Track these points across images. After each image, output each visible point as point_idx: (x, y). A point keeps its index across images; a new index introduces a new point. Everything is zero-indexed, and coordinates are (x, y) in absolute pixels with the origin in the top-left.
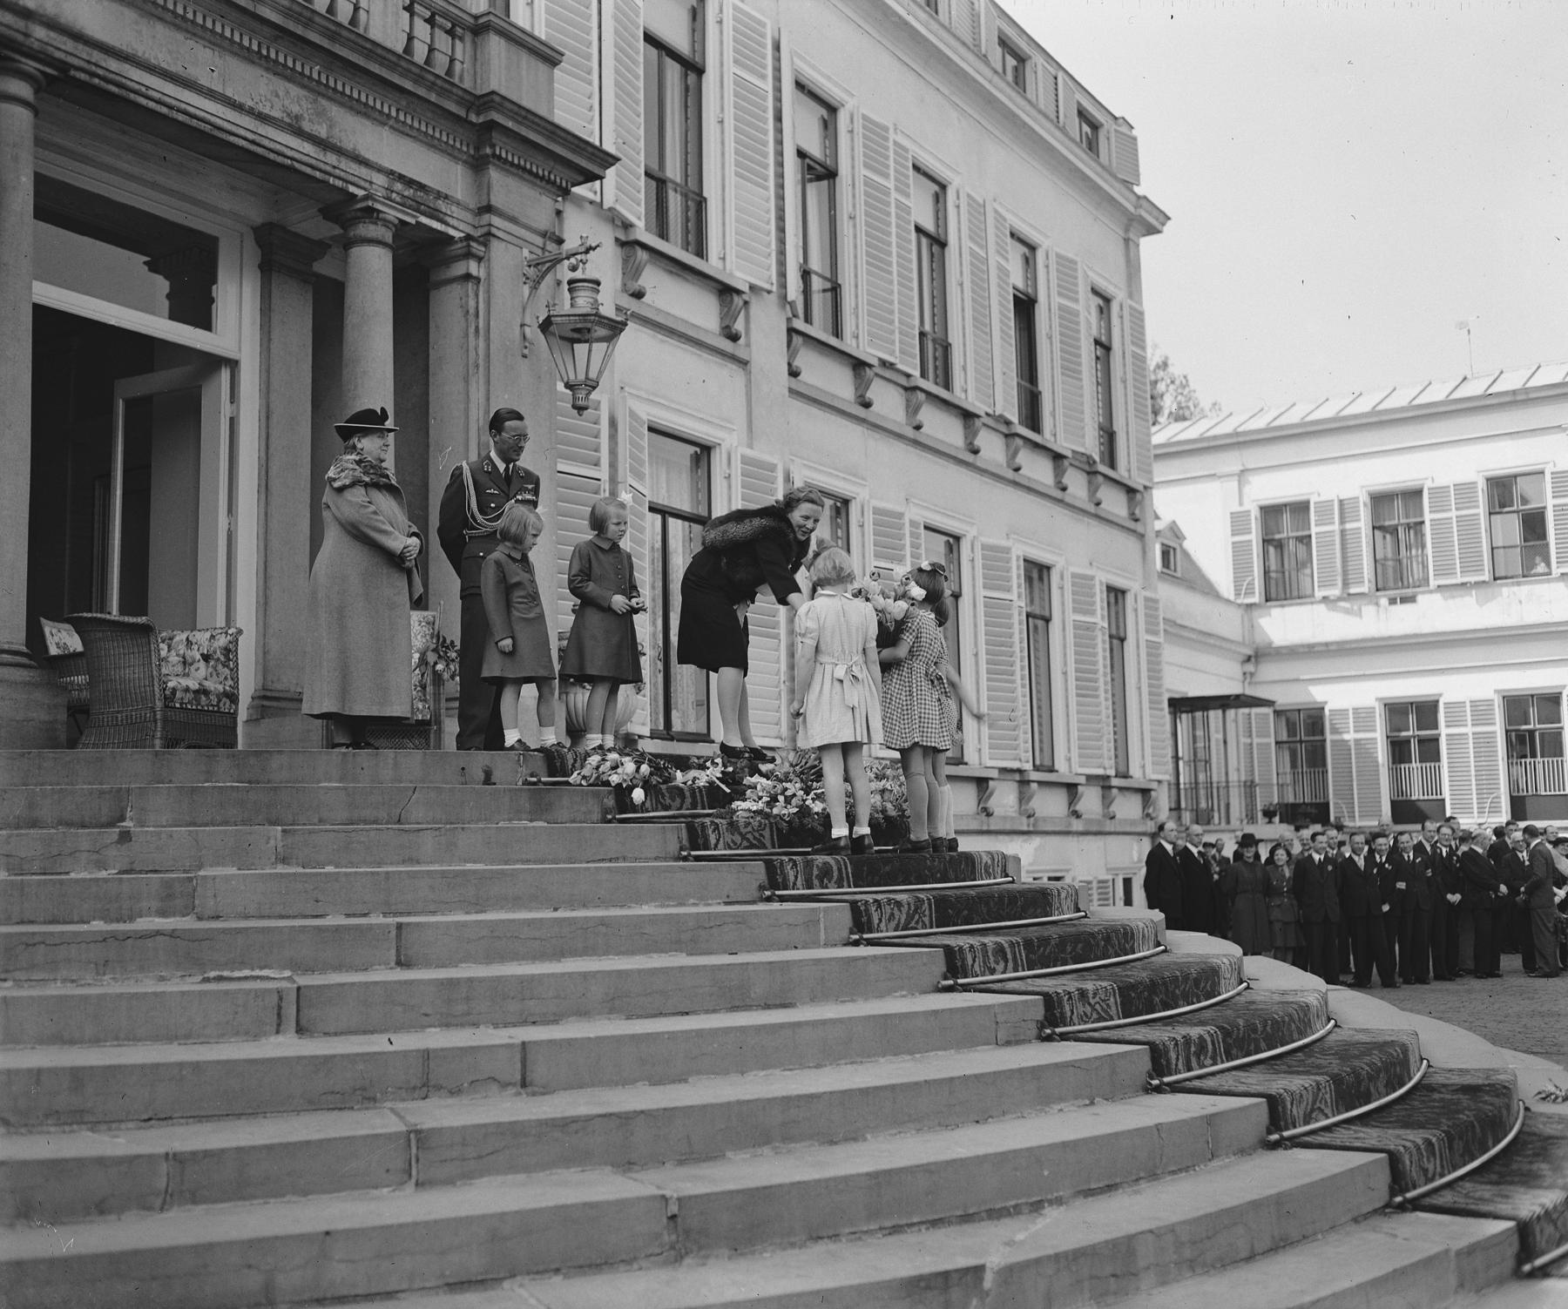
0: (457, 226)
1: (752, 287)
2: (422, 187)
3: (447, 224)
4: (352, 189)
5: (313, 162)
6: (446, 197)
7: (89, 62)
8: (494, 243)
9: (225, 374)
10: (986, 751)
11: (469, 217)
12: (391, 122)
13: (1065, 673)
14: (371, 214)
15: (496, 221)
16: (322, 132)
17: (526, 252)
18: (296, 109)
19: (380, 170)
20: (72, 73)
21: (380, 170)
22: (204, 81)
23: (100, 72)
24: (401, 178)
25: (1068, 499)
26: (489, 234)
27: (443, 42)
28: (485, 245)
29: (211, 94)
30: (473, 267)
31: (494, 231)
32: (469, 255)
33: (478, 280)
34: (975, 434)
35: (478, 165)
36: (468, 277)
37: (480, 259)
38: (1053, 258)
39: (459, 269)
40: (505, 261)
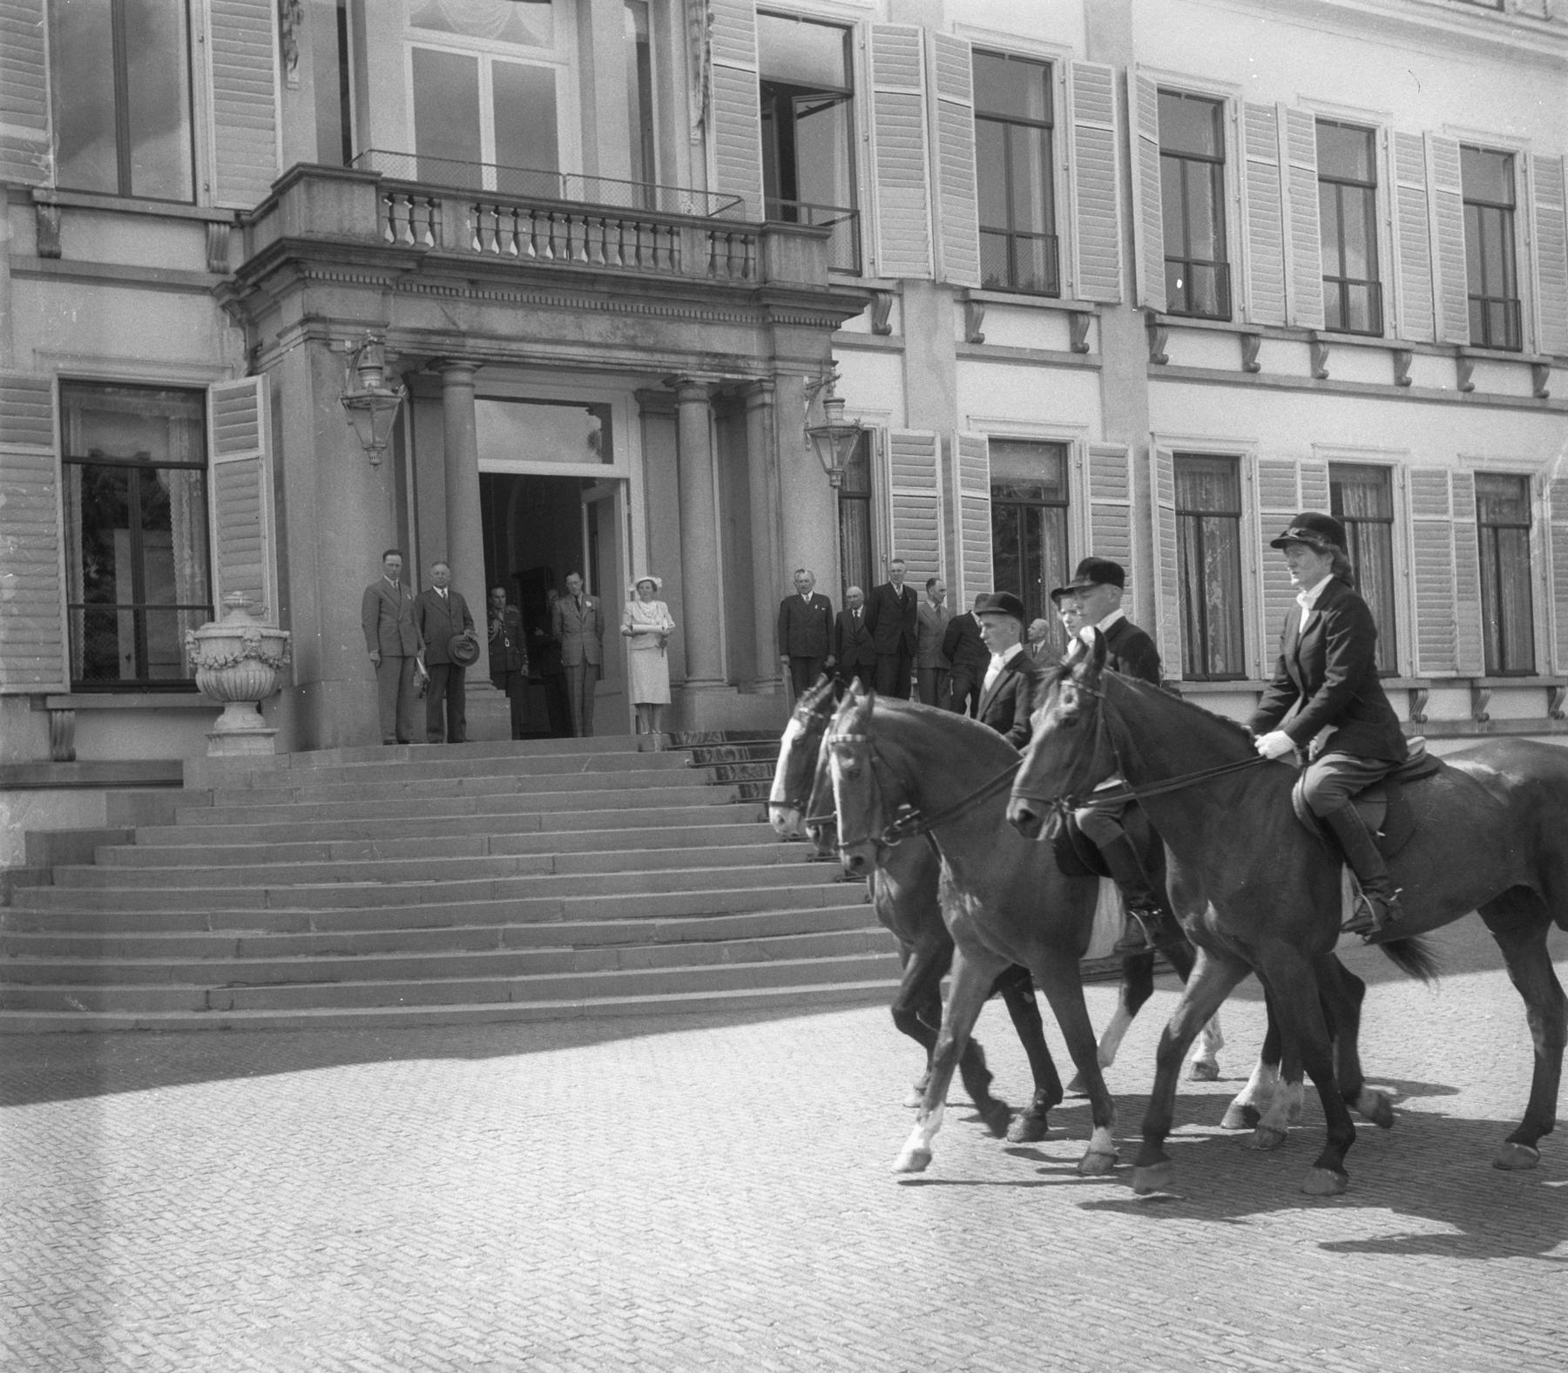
1: (1099, 304)
2: (724, 356)
6: (744, 357)
9: (623, 489)
10: (1417, 663)
11: (761, 365)
13: (1545, 579)
14: (688, 383)
15: (779, 364)
16: (650, 341)
17: (806, 379)
18: (632, 332)
22: (570, 337)
24: (708, 354)
25: (1552, 405)
27: (738, 250)
29: (574, 343)
30: (767, 398)
32: (762, 391)
33: (771, 406)
34: (1406, 366)
35: (767, 327)
36: (764, 405)
37: (771, 391)
38: (1530, 161)
39: (758, 400)
40: (791, 391)
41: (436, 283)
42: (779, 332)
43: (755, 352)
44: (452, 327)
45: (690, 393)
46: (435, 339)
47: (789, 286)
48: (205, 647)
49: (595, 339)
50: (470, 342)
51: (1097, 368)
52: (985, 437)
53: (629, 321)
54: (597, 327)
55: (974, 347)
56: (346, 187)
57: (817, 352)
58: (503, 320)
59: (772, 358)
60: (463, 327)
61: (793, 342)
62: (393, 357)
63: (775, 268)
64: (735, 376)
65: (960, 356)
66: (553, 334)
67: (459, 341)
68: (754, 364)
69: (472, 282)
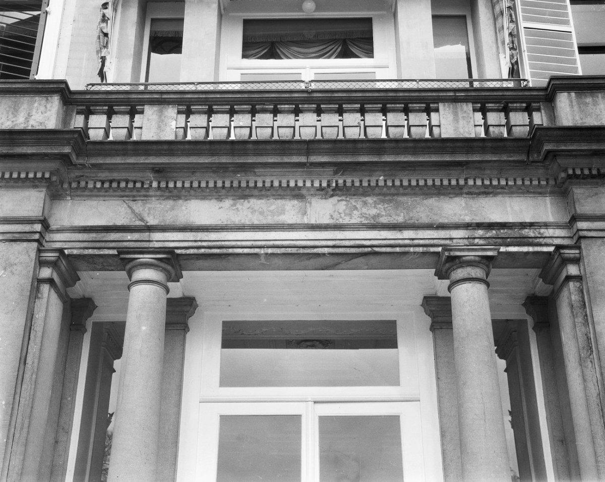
2: (503, 225)
3: (541, 245)
4: (432, 249)
5: (392, 242)
6: (531, 225)
7: (195, 241)
8: (583, 243)
12: (465, 190)
18: (374, 212)
19: (457, 226)
20: (178, 251)
21: (457, 226)
23: (204, 244)
24: (479, 226)
26: (580, 238)
28: (579, 248)
30: (573, 270)
31: (582, 233)
33: (579, 278)
36: (569, 278)
37: (577, 261)
41: (115, 175)
42: (578, 192)
43: (551, 219)
44: (138, 223)
49: (326, 220)
53: (370, 200)
60: (152, 221)
62: (51, 256)
64: (525, 249)
66: (270, 220)
67: (145, 236)
68: (550, 232)
69: (159, 171)
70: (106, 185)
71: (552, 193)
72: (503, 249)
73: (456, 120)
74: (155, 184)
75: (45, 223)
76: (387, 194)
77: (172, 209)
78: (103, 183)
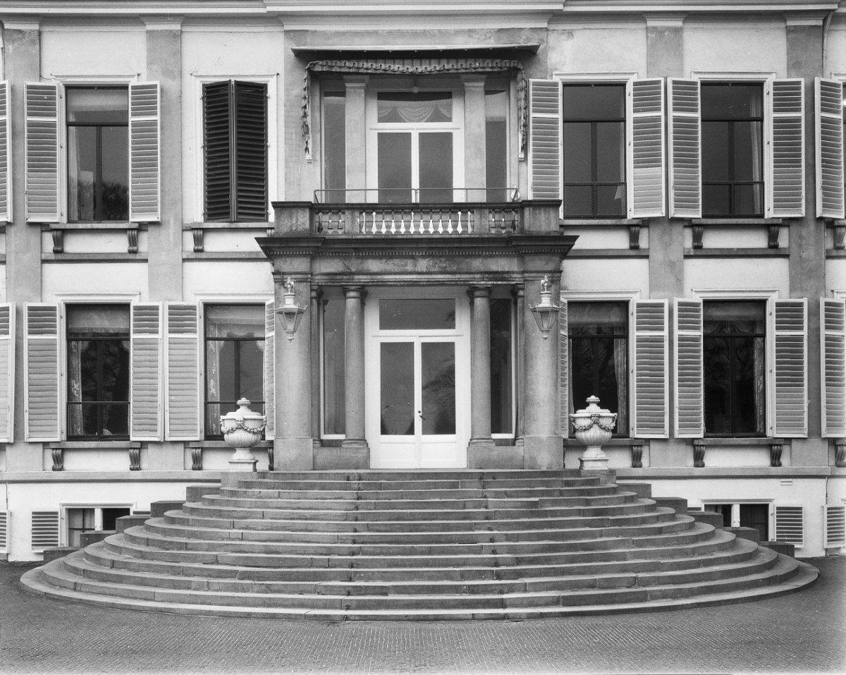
0: (517, 279)
3: (510, 281)
11: (519, 276)
15: (526, 275)
24: (486, 273)
30: (521, 293)
33: (523, 296)
36: (520, 296)
37: (523, 289)
42: (527, 258)
43: (516, 269)
44: (348, 270)
45: (477, 293)
46: (338, 277)
47: (535, 234)
48: (226, 422)
50: (357, 277)
51: (787, 256)
52: (701, 301)
53: (443, 260)
54: (423, 264)
55: (699, 252)
56: (294, 211)
57: (551, 267)
58: (374, 265)
59: (523, 272)
60: (353, 270)
61: (537, 263)
62: (315, 287)
63: (526, 225)
65: (687, 257)
66: (401, 269)
70: (334, 254)
71: (517, 257)
72: (495, 283)
73: (481, 218)
74: (354, 254)
75: (312, 274)
76: (449, 258)
77: (361, 264)
78: (332, 253)
